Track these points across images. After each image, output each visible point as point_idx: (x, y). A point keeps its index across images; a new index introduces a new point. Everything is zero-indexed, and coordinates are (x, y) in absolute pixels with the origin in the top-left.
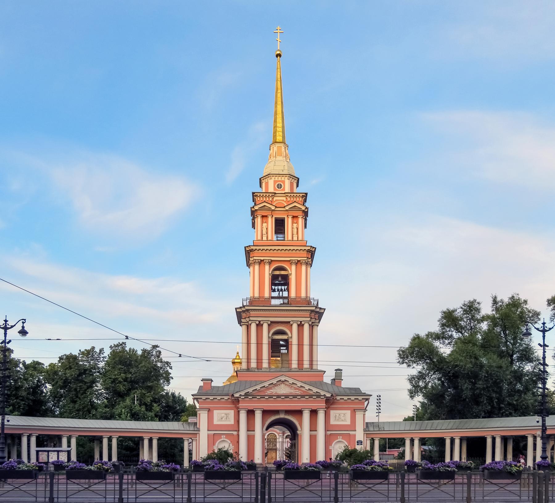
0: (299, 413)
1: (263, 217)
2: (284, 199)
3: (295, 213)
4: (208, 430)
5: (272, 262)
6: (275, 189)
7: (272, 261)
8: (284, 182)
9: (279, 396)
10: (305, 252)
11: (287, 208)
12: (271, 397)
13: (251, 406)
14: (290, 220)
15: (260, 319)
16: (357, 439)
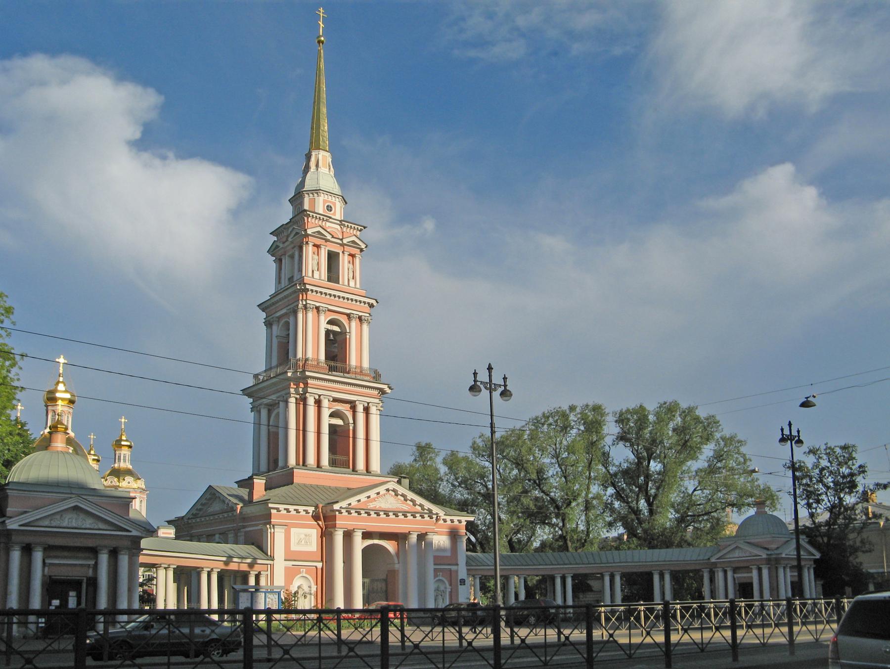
2: (338, 227)
6: (324, 211)
7: (329, 310)
10: (367, 305)
11: (345, 241)
14: (346, 257)
16: (460, 578)
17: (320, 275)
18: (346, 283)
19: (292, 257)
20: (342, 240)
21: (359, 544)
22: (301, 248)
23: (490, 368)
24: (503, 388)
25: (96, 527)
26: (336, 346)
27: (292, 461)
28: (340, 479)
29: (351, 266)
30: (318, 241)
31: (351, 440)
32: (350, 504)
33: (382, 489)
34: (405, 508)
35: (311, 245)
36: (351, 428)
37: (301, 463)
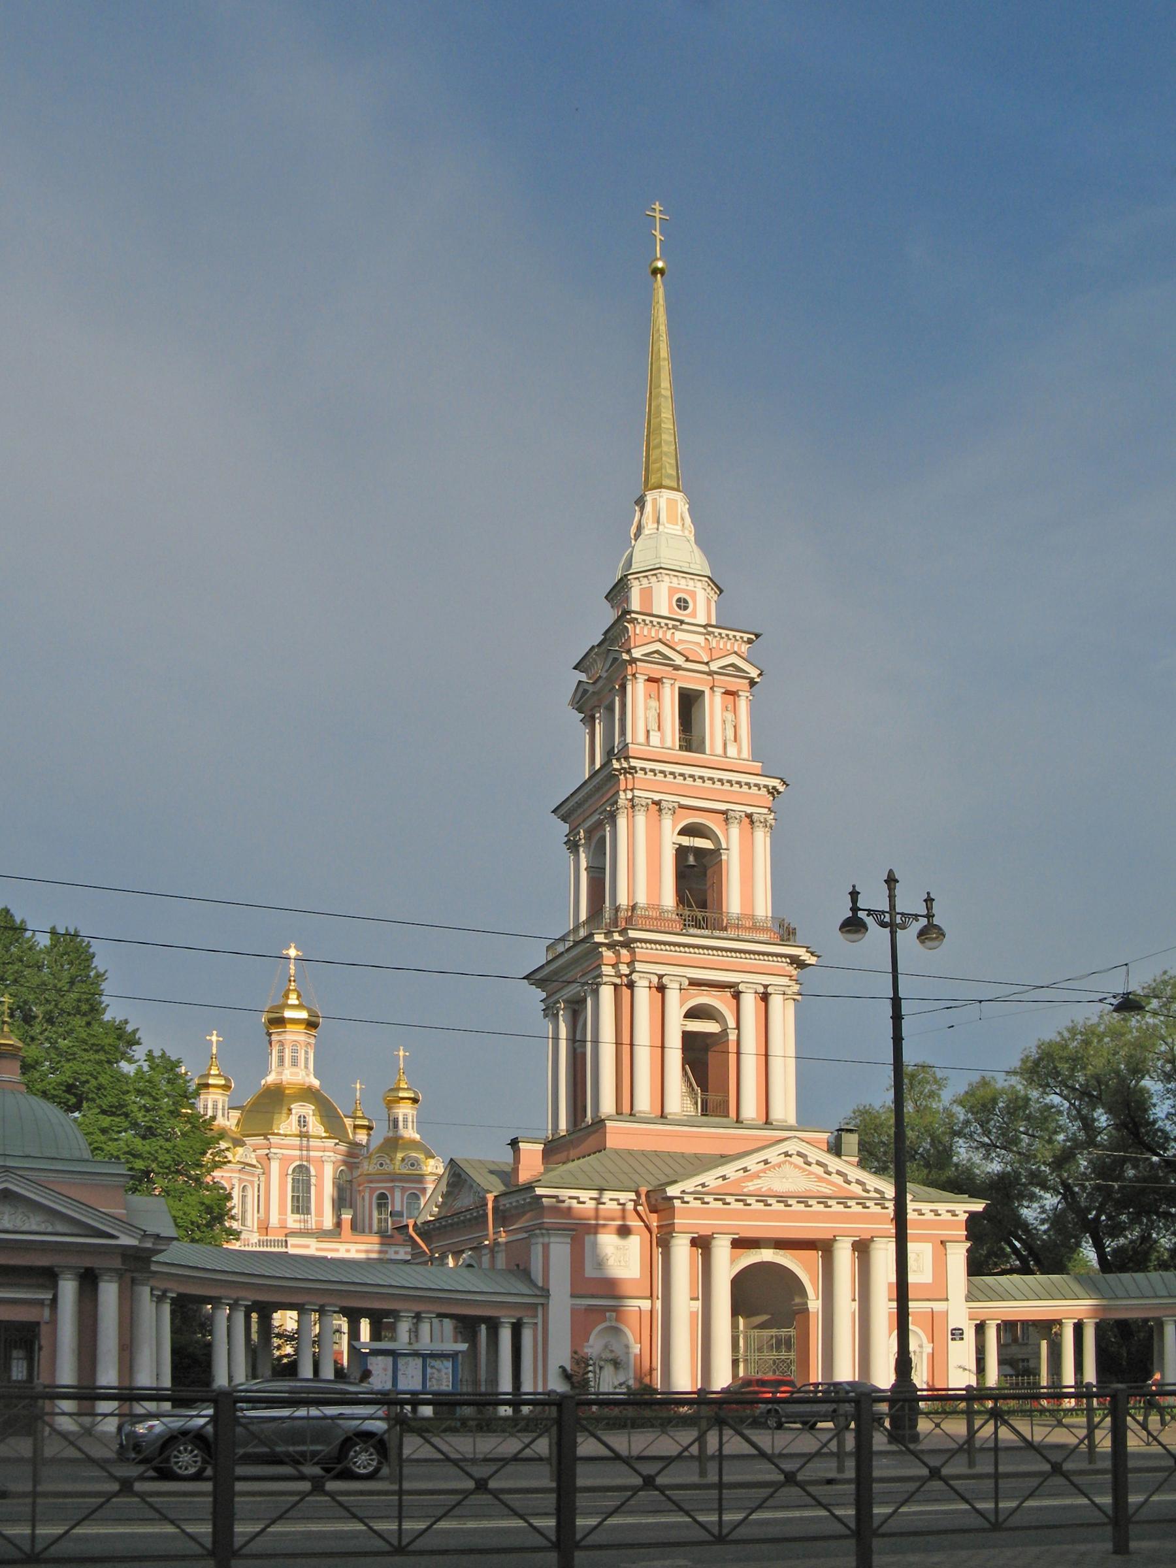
0: (825, 1247)
2: (700, 639)
4: (573, 1296)
7: (681, 807)
8: (693, 594)
9: (782, 1199)
10: (764, 791)
11: (714, 666)
12: (762, 1199)
13: (703, 1225)
14: (718, 697)
15: (661, 969)
17: (662, 740)
18: (719, 751)
19: (610, 709)
20: (707, 664)
21: (726, 1265)
22: (623, 687)
23: (891, 881)
24: (923, 922)
25: (50, 1229)
26: (697, 875)
27: (607, 1105)
28: (711, 1136)
29: (730, 716)
30: (656, 671)
31: (732, 1058)
32: (703, 1185)
33: (772, 1154)
34: (826, 1190)
35: (641, 679)
36: (732, 1037)
37: (626, 1109)
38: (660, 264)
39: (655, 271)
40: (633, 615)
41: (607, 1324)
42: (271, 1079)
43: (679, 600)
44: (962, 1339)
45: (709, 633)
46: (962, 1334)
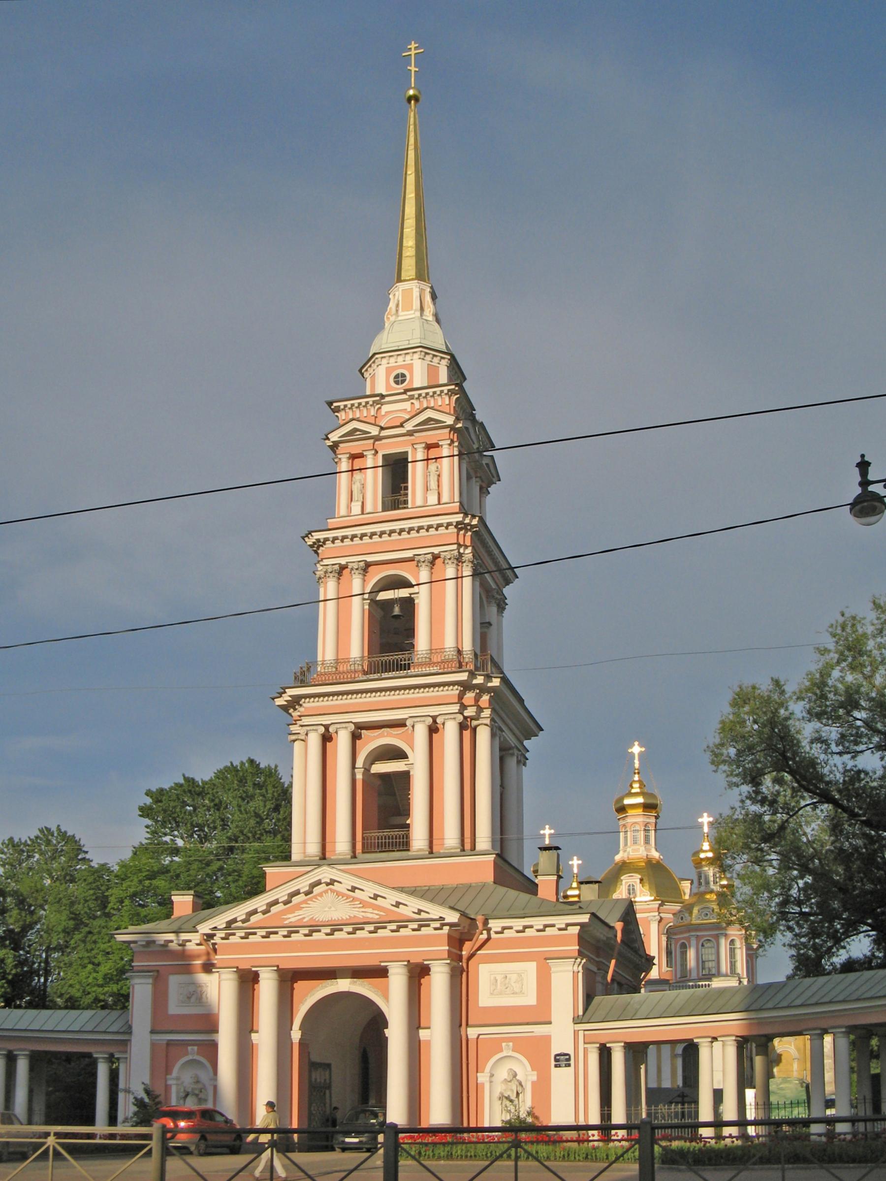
1: (353, 457)
2: (407, 405)
3: (431, 436)
5: (370, 569)
7: (368, 565)
8: (410, 367)
11: (409, 426)
13: (246, 960)
15: (326, 720)
16: (555, 1050)
20: (401, 426)
30: (355, 447)
38: (411, 92)
39: (409, 99)
40: (335, 404)
41: (190, 1057)
42: (618, 858)
43: (403, 375)
44: (569, 1065)
45: (412, 397)
46: (569, 1060)
